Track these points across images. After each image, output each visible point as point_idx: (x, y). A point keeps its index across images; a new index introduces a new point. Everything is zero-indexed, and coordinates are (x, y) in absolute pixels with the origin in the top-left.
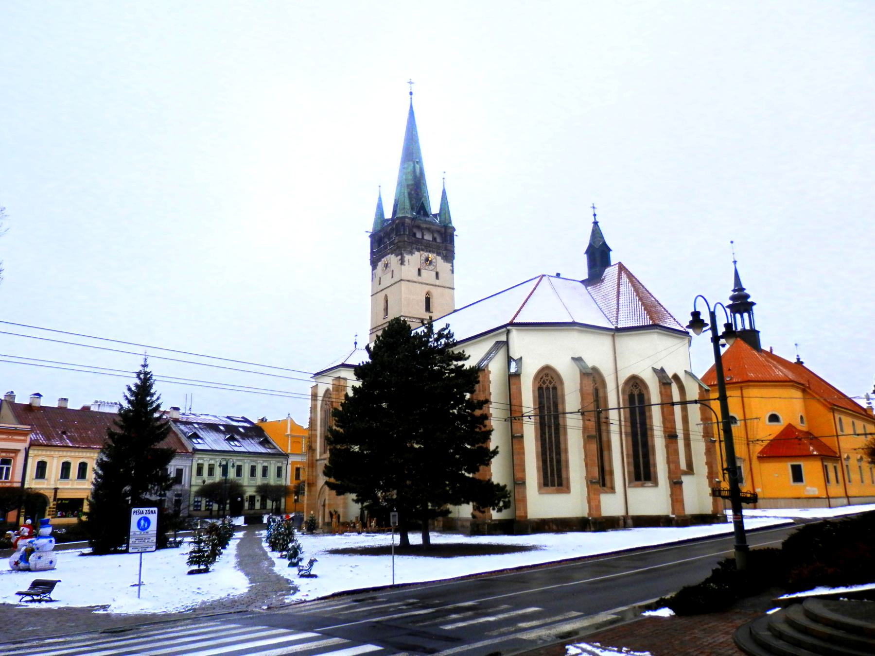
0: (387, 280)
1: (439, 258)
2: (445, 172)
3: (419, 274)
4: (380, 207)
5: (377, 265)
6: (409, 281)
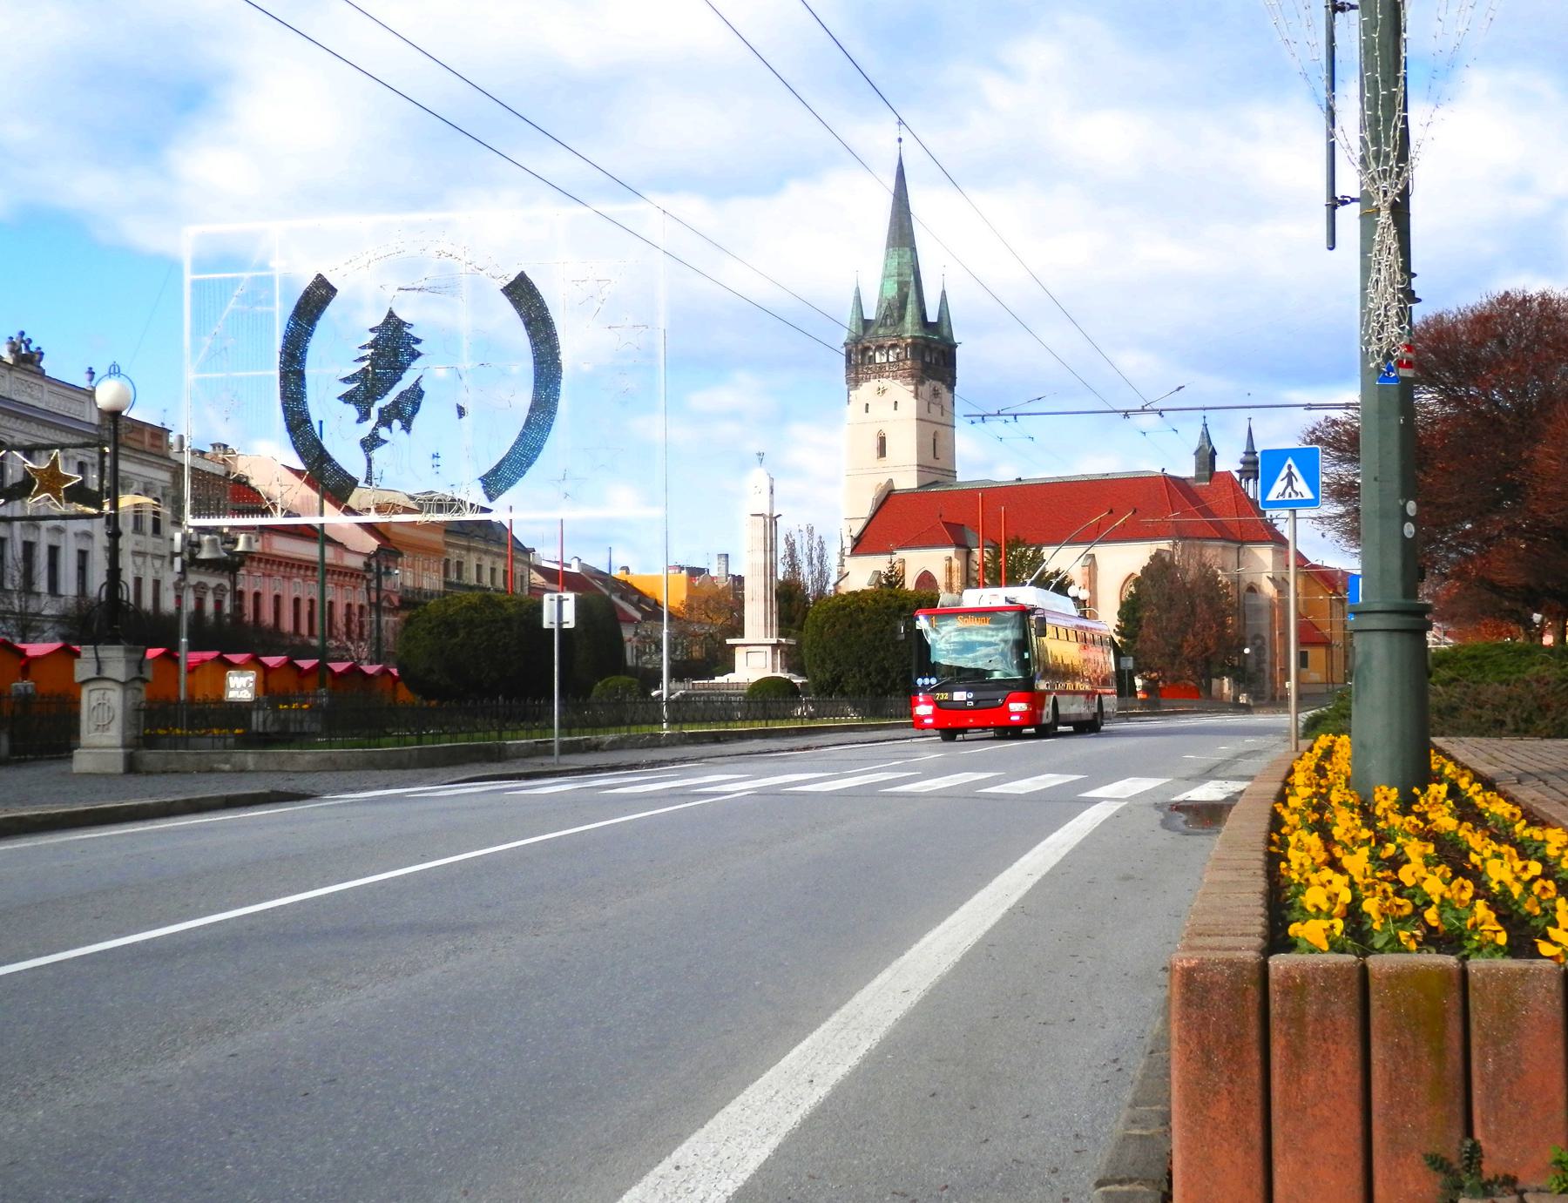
0: (881, 409)
3: (929, 411)
4: (858, 299)
6: (921, 420)
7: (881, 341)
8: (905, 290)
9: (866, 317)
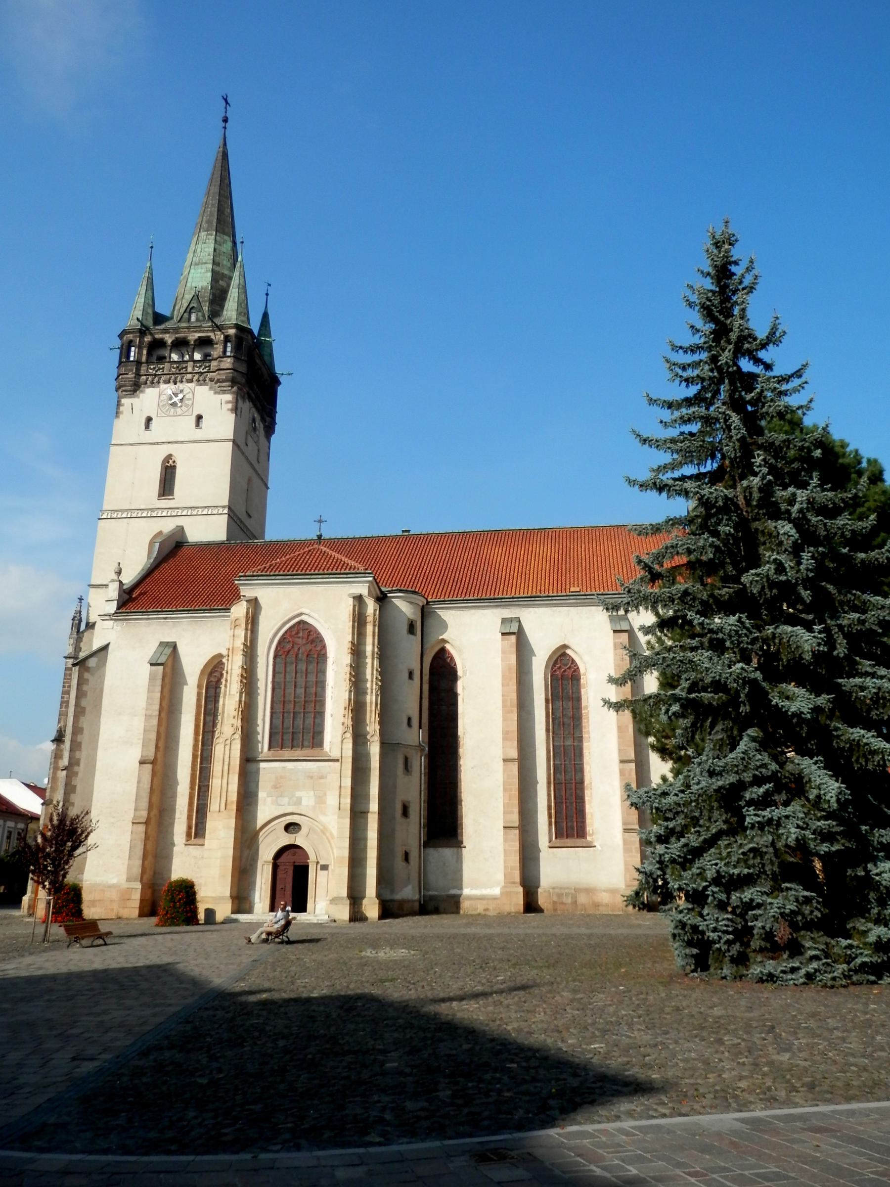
1: (262, 425)
2: (269, 285)
5: (143, 392)
7: (182, 335)
8: (221, 282)
9: (158, 310)
